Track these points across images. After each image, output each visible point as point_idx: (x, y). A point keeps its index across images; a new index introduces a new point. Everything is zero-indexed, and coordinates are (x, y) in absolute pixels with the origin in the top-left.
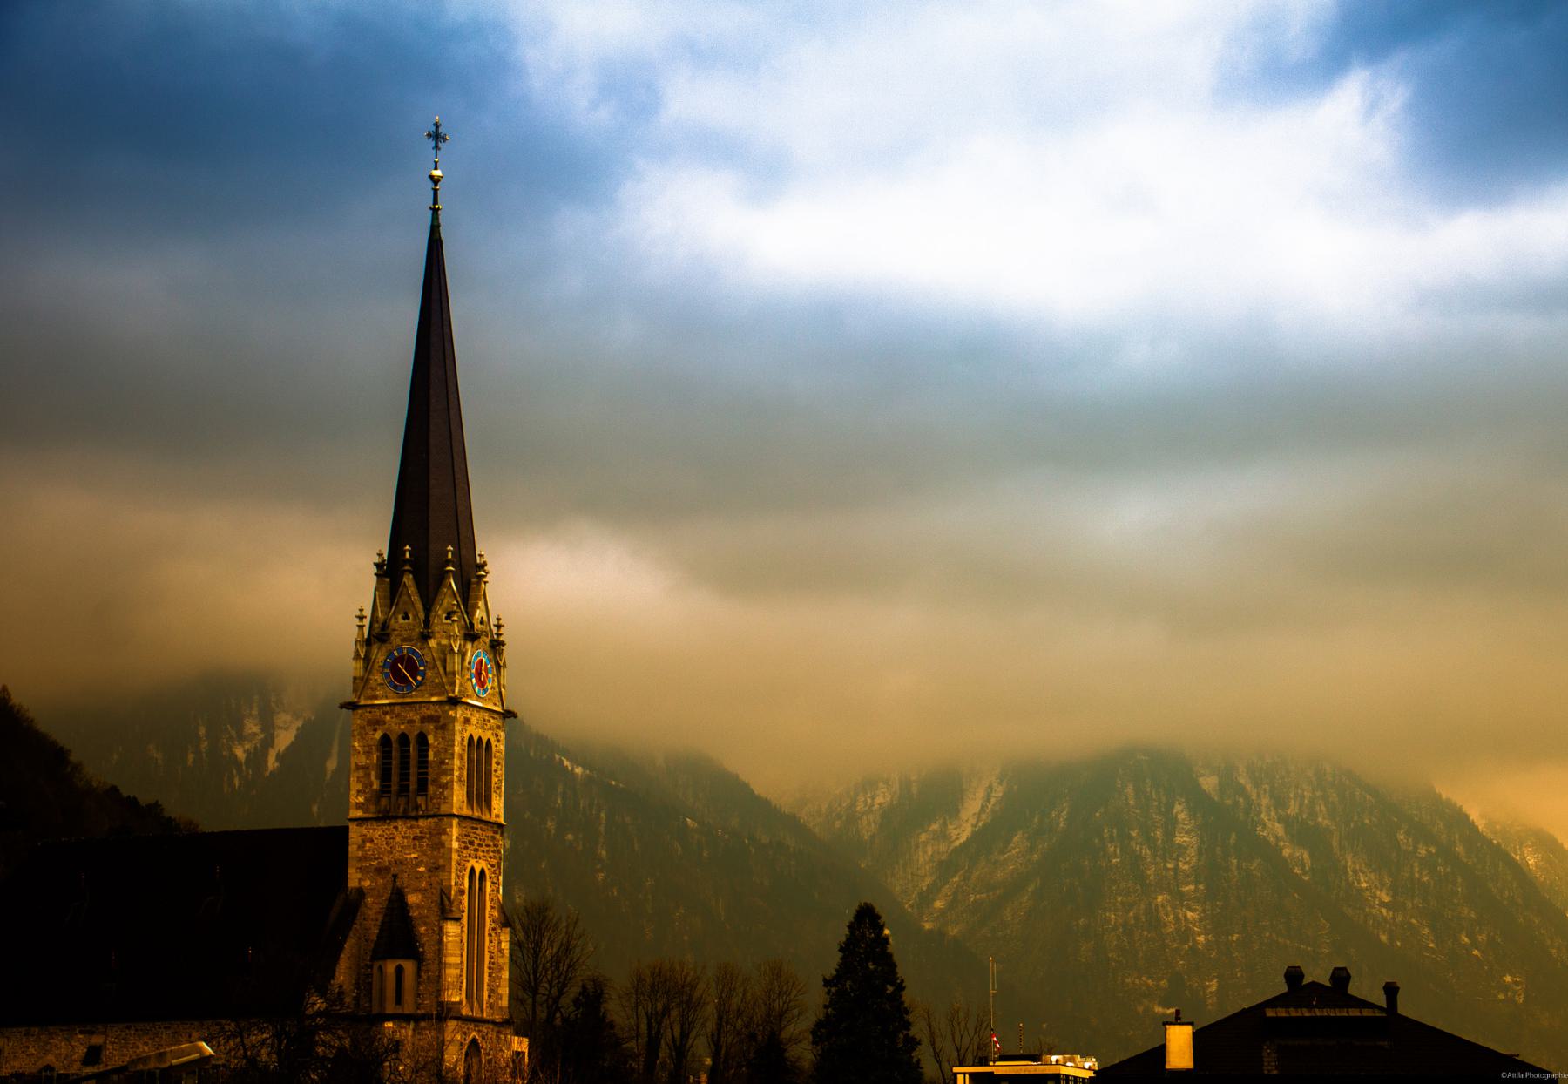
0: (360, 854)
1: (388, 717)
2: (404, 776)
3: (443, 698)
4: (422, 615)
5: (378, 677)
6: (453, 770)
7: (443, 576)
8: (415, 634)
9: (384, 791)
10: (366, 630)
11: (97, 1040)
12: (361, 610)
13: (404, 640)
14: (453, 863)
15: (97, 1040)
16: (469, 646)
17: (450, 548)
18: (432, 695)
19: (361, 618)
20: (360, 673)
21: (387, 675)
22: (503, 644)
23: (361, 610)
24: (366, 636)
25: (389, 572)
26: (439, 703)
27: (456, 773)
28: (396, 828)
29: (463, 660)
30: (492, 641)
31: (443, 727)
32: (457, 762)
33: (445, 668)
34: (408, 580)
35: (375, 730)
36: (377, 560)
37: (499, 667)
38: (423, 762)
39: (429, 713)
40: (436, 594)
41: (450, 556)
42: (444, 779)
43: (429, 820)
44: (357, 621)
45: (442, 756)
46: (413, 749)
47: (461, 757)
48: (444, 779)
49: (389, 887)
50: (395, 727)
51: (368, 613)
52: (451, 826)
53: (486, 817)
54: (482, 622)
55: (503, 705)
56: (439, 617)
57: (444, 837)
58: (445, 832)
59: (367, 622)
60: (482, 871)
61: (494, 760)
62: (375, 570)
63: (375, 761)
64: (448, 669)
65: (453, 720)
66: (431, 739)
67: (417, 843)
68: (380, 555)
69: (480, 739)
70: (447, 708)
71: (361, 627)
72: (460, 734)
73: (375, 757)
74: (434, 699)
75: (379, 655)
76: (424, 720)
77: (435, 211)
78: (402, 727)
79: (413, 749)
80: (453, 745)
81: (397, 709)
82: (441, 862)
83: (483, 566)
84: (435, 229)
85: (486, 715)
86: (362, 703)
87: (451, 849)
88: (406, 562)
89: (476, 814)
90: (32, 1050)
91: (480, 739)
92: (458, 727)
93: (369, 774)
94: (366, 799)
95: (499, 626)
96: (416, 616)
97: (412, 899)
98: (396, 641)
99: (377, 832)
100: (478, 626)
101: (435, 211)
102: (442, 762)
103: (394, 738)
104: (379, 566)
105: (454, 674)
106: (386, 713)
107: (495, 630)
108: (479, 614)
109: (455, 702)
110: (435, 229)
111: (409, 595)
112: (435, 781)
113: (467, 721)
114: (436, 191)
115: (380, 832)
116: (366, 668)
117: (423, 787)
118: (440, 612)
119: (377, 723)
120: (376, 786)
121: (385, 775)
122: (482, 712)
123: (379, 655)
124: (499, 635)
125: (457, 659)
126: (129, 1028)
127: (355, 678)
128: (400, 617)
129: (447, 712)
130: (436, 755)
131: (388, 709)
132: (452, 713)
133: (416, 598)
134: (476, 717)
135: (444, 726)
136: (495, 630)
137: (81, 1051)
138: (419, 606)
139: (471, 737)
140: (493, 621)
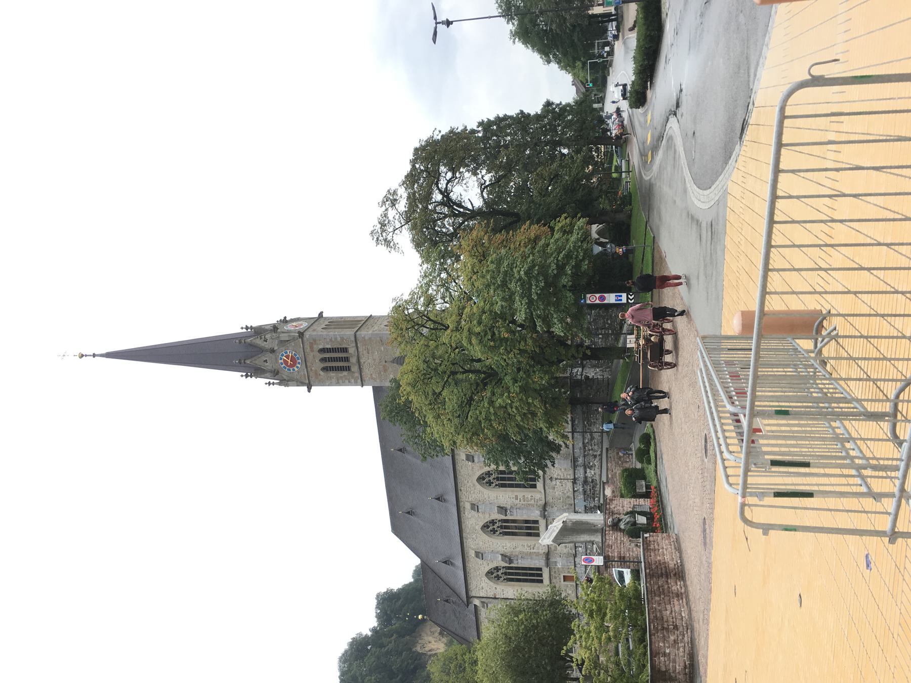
0: (378, 380)
1: (313, 369)
3: (300, 340)
6: (334, 335)
9: (348, 369)
10: (276, 381)
11: (468, 506)
12: (266, 384)
14: (379, 332)
15: (468, 506)
16: (279, 330)
23: (266, 384)
24: (278, 381)
25: (255, 371)
28: (364, 362)
31: (315, 340)
32: (332, 333)
33: (288, 341)
35: (320, 375)
36: (244, 377)
39: (309, 348)
42: (339, 339)
43: (358, 345)
46: (327, 355)
48: (339, 339)
49: (393, 364)
50: (317, 365)
51: (267, 381)
52: (361, 334)
56: (265, 345)
57: (366, 338)
58: (364, 338)
59: (272, 381)
62: (249, 377)
63: (334, 374)
65: (310, 336)
66: (321, 347)
67: (370, 352)
68: (242, 376)
70: (305, 339)
71: (273, 384)
73: (332, 374)
76: (312, 351)
77: (94, 355)
78: (317, 361)
79: (327, 355)
81: (308, 364)
82: (378, 339)
84: (102, 355)
86: (307, 382)
87: (372, 334)
90: (474, 536)
93: (341, 377)
94: (353, 377)
97: (397, 354)
99: (367, 372)
101: (94, 355)
102: (331, 340)
104: (247, 376)
105: (289, 336)
106: (311, 369)
108: (267, 328)
110: (102, 355)
114: (86, 356)
115: (367, 370)
116: (293, 381)
117: (345, 350)
119: (316, 374)
120: (345, 373)
123: (285, 373)
125: (282, 335)
126: (461, 490)
127: (298, 386)
128: (265, 363)
130: (328, 344)
131: (309, 369)
135: (314, 342)
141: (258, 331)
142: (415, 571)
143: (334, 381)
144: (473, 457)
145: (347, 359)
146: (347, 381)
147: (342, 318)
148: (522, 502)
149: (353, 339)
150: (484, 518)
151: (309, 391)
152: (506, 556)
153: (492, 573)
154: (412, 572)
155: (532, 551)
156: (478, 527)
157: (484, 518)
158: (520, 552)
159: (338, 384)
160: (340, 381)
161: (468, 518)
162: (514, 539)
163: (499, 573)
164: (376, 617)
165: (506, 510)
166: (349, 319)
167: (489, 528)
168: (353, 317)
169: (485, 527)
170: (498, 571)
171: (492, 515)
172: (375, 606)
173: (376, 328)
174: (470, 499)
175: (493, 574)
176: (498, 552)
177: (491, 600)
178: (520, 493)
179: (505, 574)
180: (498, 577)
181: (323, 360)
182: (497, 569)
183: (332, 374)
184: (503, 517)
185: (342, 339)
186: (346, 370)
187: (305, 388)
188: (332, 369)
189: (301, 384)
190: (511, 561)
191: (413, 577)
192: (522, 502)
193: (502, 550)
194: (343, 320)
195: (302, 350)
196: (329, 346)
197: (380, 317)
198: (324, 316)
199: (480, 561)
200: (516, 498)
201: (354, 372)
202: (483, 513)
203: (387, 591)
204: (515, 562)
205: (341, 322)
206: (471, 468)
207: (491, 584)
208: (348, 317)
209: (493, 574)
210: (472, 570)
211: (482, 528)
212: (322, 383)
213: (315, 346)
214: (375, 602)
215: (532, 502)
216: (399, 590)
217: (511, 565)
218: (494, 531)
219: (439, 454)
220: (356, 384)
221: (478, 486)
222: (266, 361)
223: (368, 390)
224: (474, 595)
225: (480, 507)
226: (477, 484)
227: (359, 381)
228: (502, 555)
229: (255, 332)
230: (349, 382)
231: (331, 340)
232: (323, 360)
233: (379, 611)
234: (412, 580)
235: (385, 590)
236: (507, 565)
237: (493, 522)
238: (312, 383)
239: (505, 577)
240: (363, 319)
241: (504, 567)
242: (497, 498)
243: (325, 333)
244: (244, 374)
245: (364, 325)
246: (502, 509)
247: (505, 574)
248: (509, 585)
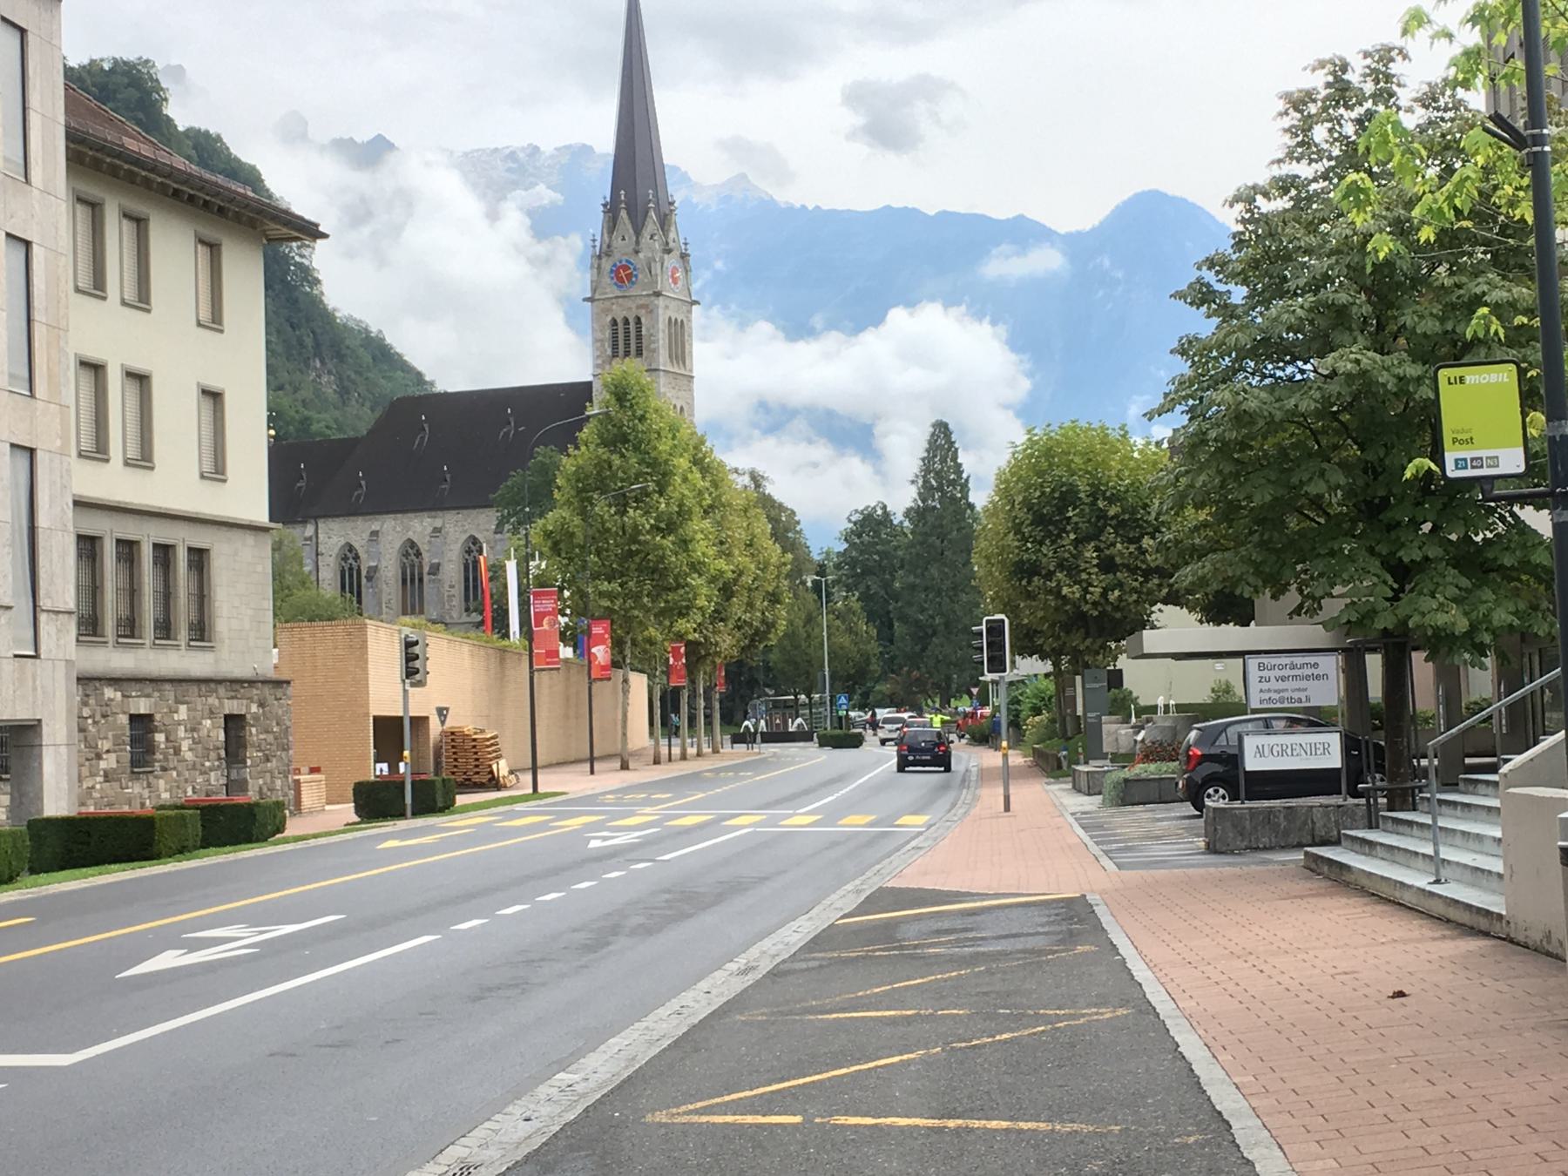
1: (614, 307)
2: (627, 345)
3: (651, 292)
4: (634, 239)
5: (608, 280)
7: (647, 212)
8: (630, 249)
9: (615, 355)
10: (598, 249)
11: (438, 523)
13: (623, 254)
15: (438, 523)
16: (666, 256)
17: (650, 191)
18: (644, 290)
19: (594, 241)
20: (595, 278)
21: (612, 278)
22: (688, 255)
25: (611, 210)
26: (648, 295)
27: (661, 342)
29: (662, 264)
30: (682, 253)
31: (651, 312)
32: (661, 335)
34: (623, 214)
37: (687, 271)
38: (639, 337)
40: (643, 224)
41: (651, 197)
42: (652, 346)
44: (591, 243)
45: (652, 331)
46: (632, 326)
47: (664, 331)
48: (652, 346)
51: (598, 238)
52: (659, 377)
53: (683, 372)
54: (674, 241)
55: (691, 297)
59: (598, 244)
60: (682, 409)
61: (686, 334)
62: (602, 208)
64: (653, 273)
66: (643, 320)
68: (605, 198)
69: (676, 320)
70: (653, 298)
72: (663, 317)
74: (644, 293)
75: (607, 265)
76: (639, 307)
79: (632, 326)
80: (658, 323)
81: (620, 300)
83: (672, 204)
85: (680, 303)
86: (597, 297)
88: (621, 202)
89: (676, 370)
90: (398, 529)
91: (676, 320)
92: (661, 311)
93: (603, 346)
94: (604, 362)
95: (686, 244)
96: (630, 238)
98: (617, 256)
100: (671, 245)
102: (651, 335)
103: (619, 321)
104: (605, 206)
105: (656, 275)
107: (683, 247)
108: (672, 235)
109: (658, 294)
111: (625, 224)
112: (648, 346)
113: (667, 307)
116: (599, 273)
117: (639, 353)
118: (646, 234)
119: (607, 311)
120: (609, 352)
121: (615, 346)
122: (677, 302)
124: (686, 250)
125: (659, 265)
127: (592, 282)
128: (621, 238)
129: (652, 302)
130: (648, 330)
131: (614, 301)
132: (656, 302)
133: (629, 227)
134: (673, 304)
135: (652, 312)
136: (683, 247)
137: (430, 529)
138: (631, 231)
139: (670, 319)
140: (682, 241)
141: (665, 221)
142: (207, 134)
143: (600, 336)
144: (501, 533)
145: (627, 354)
146: (598, 353)
147: (690, 335)
148: (446, 594)
149: (653, 367)
150: (423, 543)
151: (585, 300)
152: (375, 572)
153: (350, 551)
154: (203, 128)
155: (384, 606)
156: (410, 535)
157: (423, 543)
158: (381, 591)
159: (596, 341)
160: (599, 344)
161: (422, 522)
162: (397, 581)
163: (351, 561)
164: (93, 62)
165: (434, 574)
166: (687, 346)
167: (411, 550)
168: (691, 352)
169: (412, 544)
170: (354, 558)
171: (428, 554)
172: (117, 56)
173: (669, 395)
174: (447, 526)
175: (349, 553)
176: (379, 561)
177: (315, 548)
178: (459, 591)
179: (351, 569)
180: (345, 559)
181: (626, 322)
182: (357, 558)
183: (608, 333)
184: (426, 569)
185: (654, 351)
186: (613, 352)
187: (589, 295)
188: (615, 334)
189: (594, 290)
190: (369, 579)
191: (189, 130)
192: (446, 594)
193: (384, 564)
194: (686, 337)
195: (639, 293)
196: (643, 329)
197: (691, 390)
198: (694, 307)
199: (366, 536)
200: (452, 586)
201: (610, 363)
202: (430, 542)
203: (162, 89)
204: (369, 584)
205: (683, 335)
206: (487, 526)
207: (336, 550)
208: (691, 345)
209: (349, 553)
210: (352, 524)
211: (409, 539)
212: (596, 318)
213: (644, 311)
214: (130, 56)
215: (447, 607)
216: (169, 120)
217: (364, 581)
218: (406, 555)
219: (499, 514)
220: (597, 366)
221: (465, 537)
222: (624, 239)
223: (590, 378)
224: (320, 525)
225: (438, 540)
226: (468, 535)
227: (599, 371)
228: (376, 567)
229: (666, 215)
230: (598, 357)
231: (651, 335)
232: (626, 322)
233: (106, 66)
234: (181, 129)
235: (164, 85)
236: (364, 573)
237: (418, 554)
238: (596, 303)
239: (346, 568)
240: (688, 368)
241: (359, 567)
242: (450, 561)
243: (662, 325)
244: (608, 200)
245: (675, 376)
246: (435, 569)
247: (351, 569)
248: (335, 574)
